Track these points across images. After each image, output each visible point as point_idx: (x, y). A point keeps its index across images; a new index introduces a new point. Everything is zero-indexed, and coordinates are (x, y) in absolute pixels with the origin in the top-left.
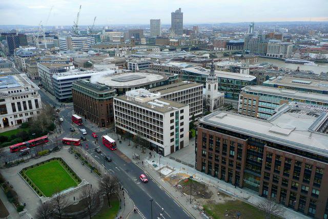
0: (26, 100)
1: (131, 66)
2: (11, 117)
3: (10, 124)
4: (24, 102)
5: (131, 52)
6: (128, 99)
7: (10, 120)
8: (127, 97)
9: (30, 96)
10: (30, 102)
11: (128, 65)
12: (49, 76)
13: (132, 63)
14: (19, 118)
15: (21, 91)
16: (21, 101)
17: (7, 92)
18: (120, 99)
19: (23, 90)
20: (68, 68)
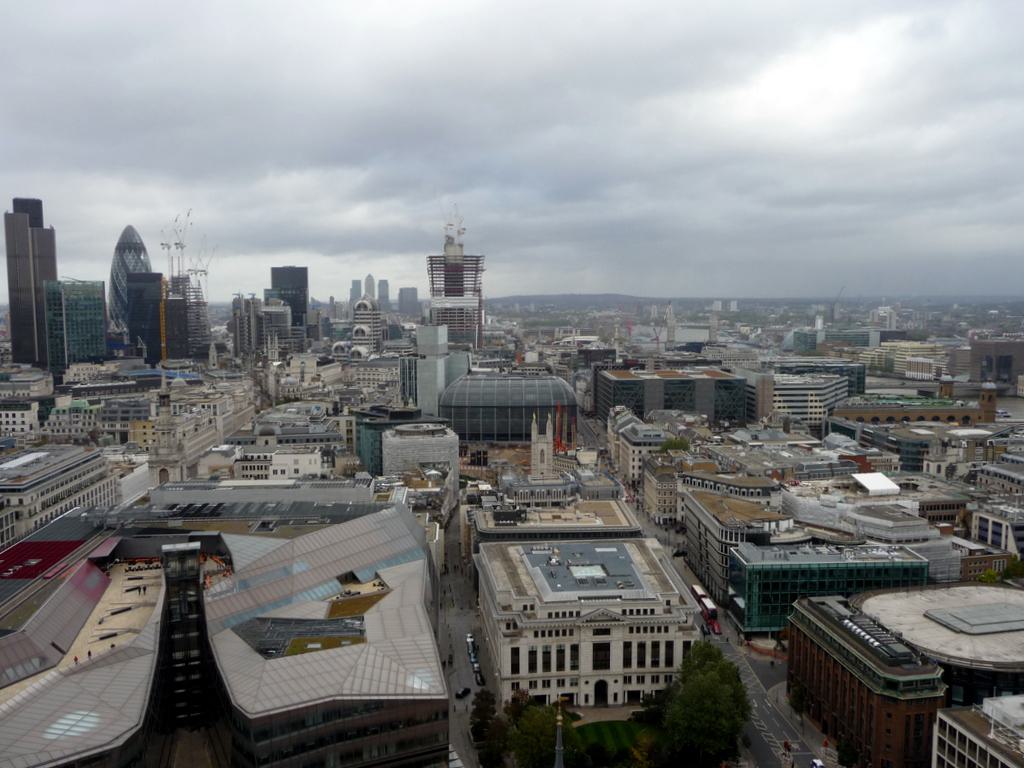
0: (662, 638)
1: (983, 529)
2: (616, 681)
3: (610, 700)
4: (656, 645)
5: (980, 450)
6: (991, 736)
7: (612, 689)
8: (986, 721)
9: (672, 629)
10: (670, 645)
11: (975, 523)
12: (717, 545)
13: (991, 519)
14: (634, 686)
15: (652, 611)
16: (648, 639)
17: (619, 611)
18: (955, 719)
19: (659, 610)
20: (773, 525)
